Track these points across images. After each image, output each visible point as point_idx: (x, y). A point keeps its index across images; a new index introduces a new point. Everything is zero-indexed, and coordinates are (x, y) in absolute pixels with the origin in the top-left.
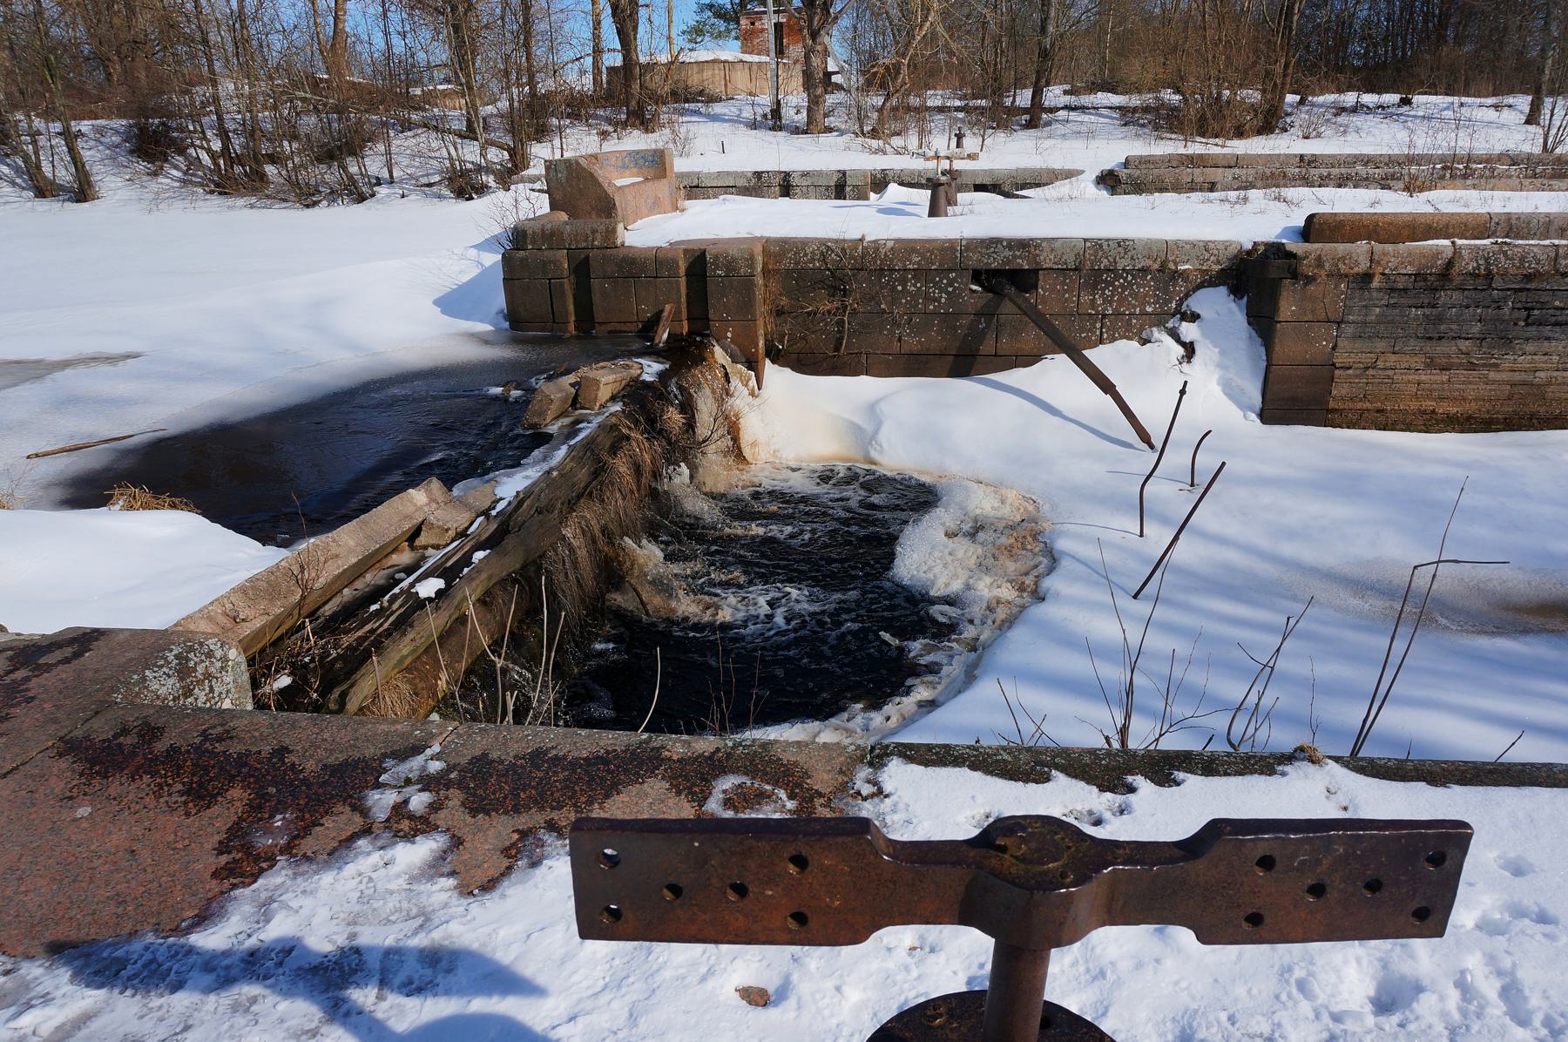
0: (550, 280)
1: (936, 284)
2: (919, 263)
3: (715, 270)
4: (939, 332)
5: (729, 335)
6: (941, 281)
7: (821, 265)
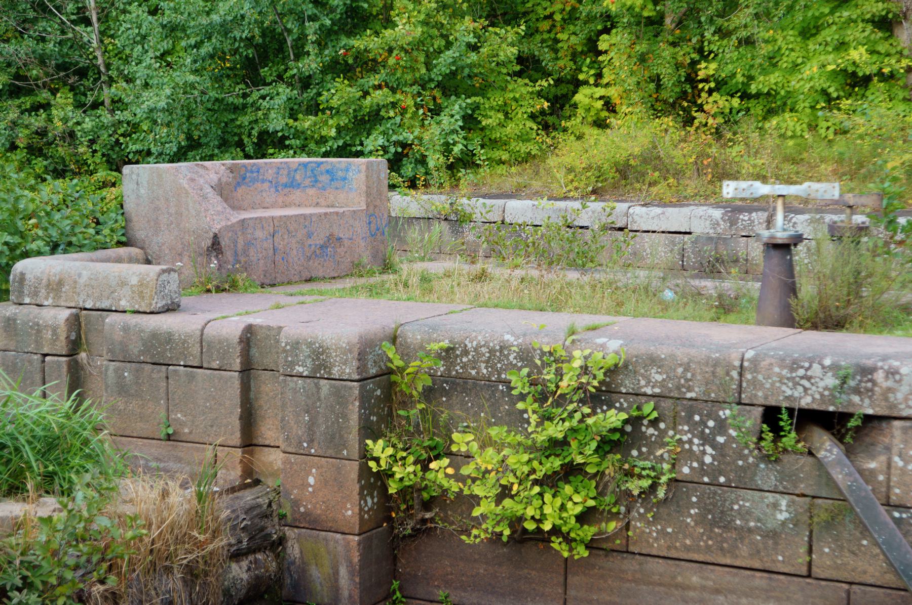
0: (45, 355)
1: (693, 425)
2: (662, 384)
3: (292, 364)
4: (700, 520)
5: (311, 480)
6: (703, 423)
7: (491, 374)
